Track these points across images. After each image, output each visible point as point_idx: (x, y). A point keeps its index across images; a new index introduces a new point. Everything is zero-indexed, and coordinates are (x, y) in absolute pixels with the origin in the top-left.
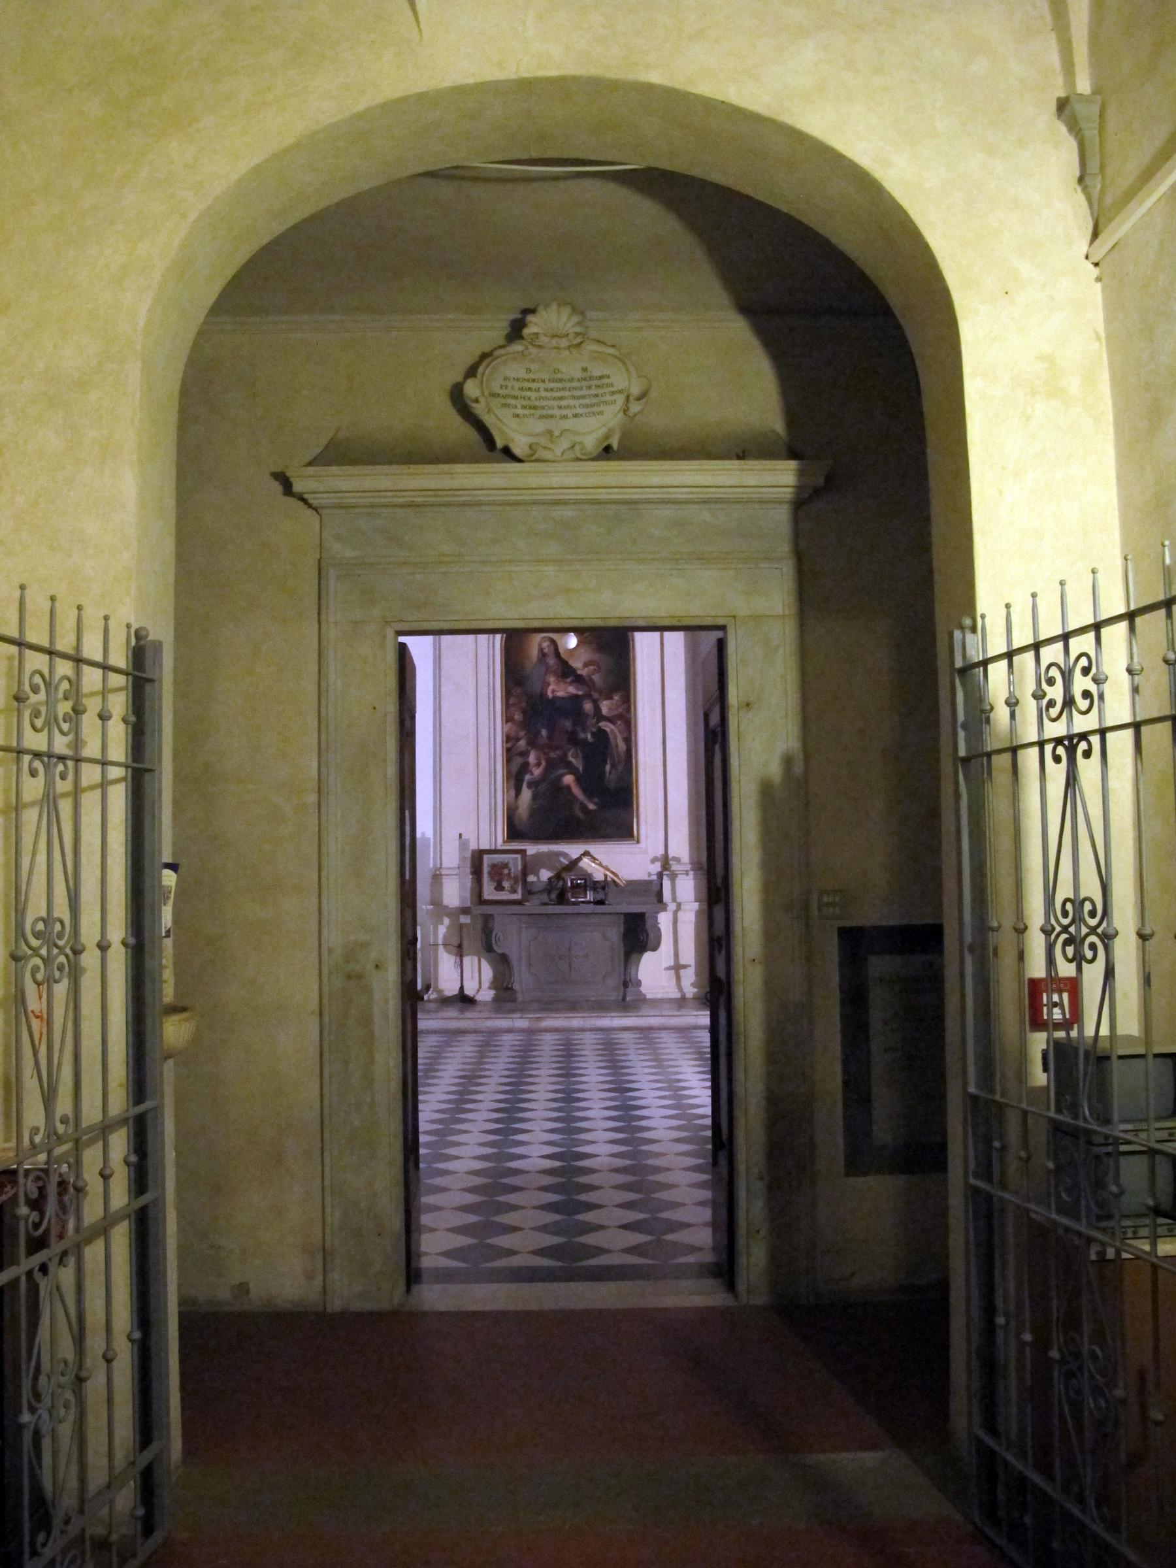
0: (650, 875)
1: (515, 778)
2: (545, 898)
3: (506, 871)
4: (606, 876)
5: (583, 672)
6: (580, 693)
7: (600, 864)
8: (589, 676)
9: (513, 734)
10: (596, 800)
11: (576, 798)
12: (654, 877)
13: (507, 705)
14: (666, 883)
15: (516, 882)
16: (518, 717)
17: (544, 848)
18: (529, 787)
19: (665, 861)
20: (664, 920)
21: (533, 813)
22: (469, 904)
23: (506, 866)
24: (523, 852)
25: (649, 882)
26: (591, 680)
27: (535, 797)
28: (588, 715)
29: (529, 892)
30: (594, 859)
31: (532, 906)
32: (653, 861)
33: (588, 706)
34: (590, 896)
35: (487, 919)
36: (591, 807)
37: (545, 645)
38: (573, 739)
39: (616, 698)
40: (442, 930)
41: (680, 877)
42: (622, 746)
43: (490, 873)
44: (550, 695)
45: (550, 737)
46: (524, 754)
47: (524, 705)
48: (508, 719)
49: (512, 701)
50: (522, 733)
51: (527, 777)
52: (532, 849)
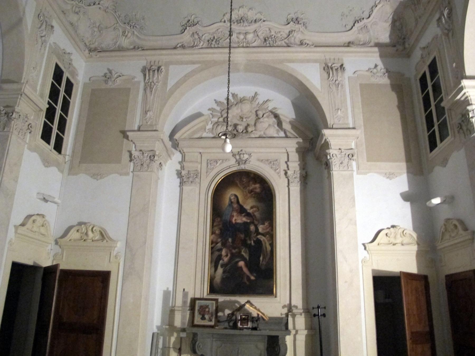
0: (281, 314)
1: (215, 261)
2: (226, 325)
3: (207, 310)
4: (258, 315)
5: (251, 211)
6: (249, 221)
7: (255, 308)
8: (253, 213)
9: (215, 240)
10: (255, 274)
11: (245, 273)
12: (284, 316)
13: (213, 226)
14: (290, 319)
15: (212, 316)
16: (217, 232)
17: (228, 298)
18: (222, 267)
19: (290, 308)
20: (289, 339)
21: (223, 280)
22: (186, 326)
23: (207, 307)
24: (216, 300)
25: (281, 319)
26: (254, 215)
27: (224, 272)
28: (251, 232)
29: (218, 321)
30: (252, 305)
31: (219, 330)
32: (284, 307)
33: (252, 228)
34: (250, 325)
35: (195, 335)
36: (252, 278)
37: (232, 198)
38: (244, 243)
39: (266, 224)
40: (173, 339)
41: (297, 316)
42: (269, 248)
43: (199, 310)
44: (234, 221)
45: (233, 242)
46: (220, 250)
47: (221, 226)
48: (213, 233)
49: (215, 224)
50: (219, 240)
51: (221, 262)
52: (221, 299)
